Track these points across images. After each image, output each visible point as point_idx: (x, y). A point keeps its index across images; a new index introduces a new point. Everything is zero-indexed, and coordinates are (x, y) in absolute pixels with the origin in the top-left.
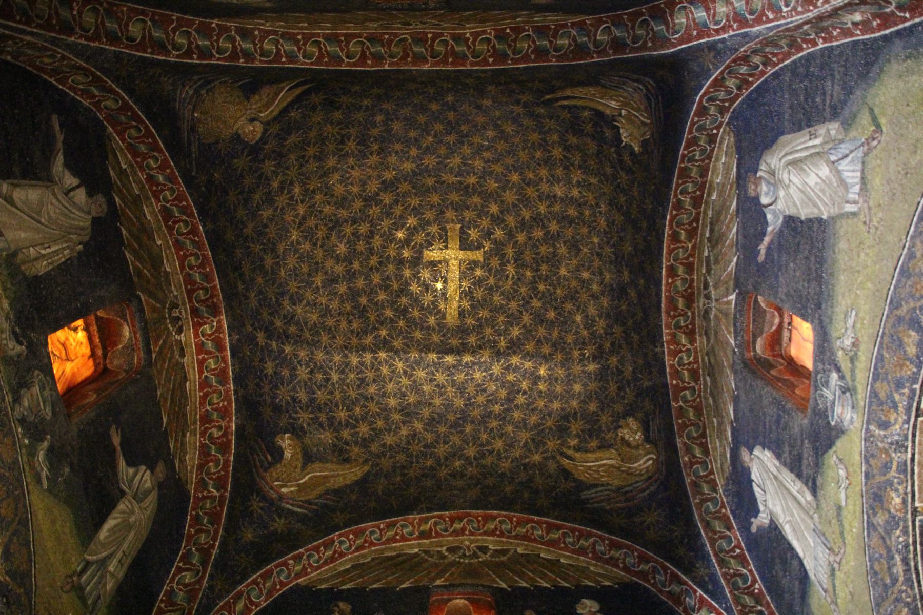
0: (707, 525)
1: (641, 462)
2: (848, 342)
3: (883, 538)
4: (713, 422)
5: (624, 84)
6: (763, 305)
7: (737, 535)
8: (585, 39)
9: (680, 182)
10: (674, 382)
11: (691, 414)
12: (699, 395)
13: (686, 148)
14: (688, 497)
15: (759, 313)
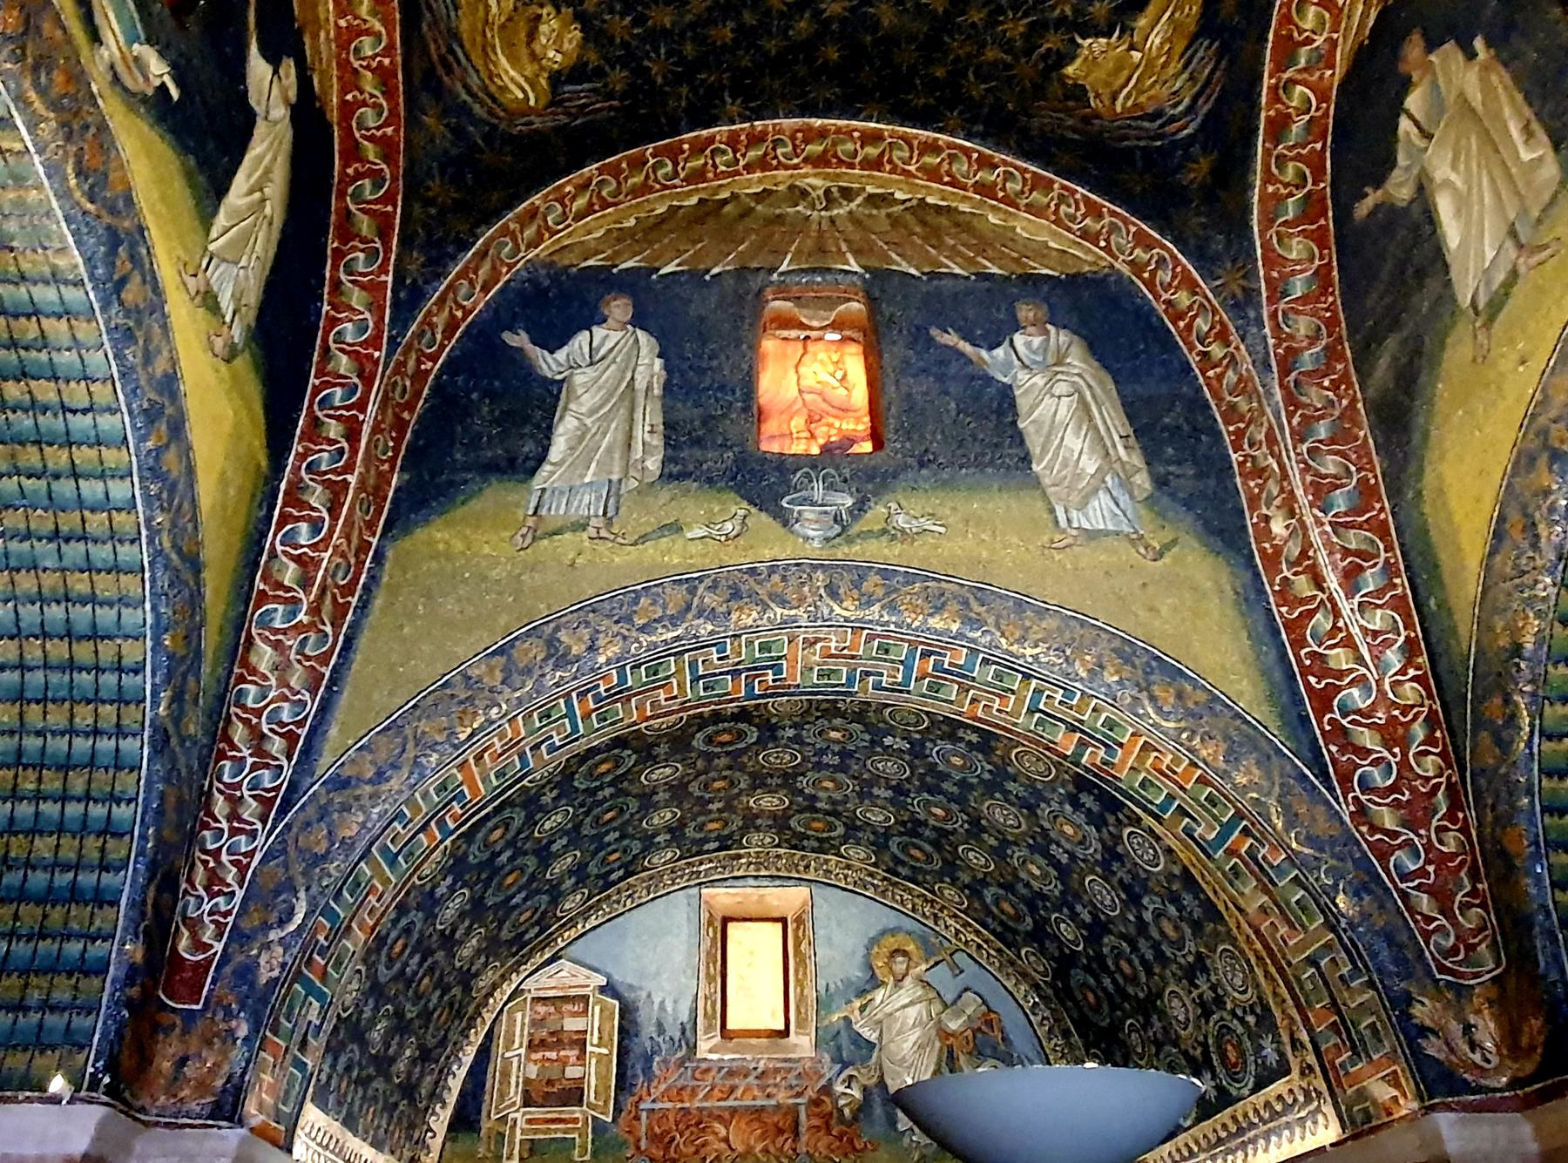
0: (482, 254)
1: (512, 73)
2: (901, 521)
3: (688, 608)
4: (627, 218)
5: (1191, 78)
6: (842, 307)
7: (479, 303)
8: (1302, 62)
9: (1028, 176)
10: (686, 146)
11: (637, 179)
12: (665, 187)
13: (1086, 200)
14: (511, 207)
15: (831, 303)
